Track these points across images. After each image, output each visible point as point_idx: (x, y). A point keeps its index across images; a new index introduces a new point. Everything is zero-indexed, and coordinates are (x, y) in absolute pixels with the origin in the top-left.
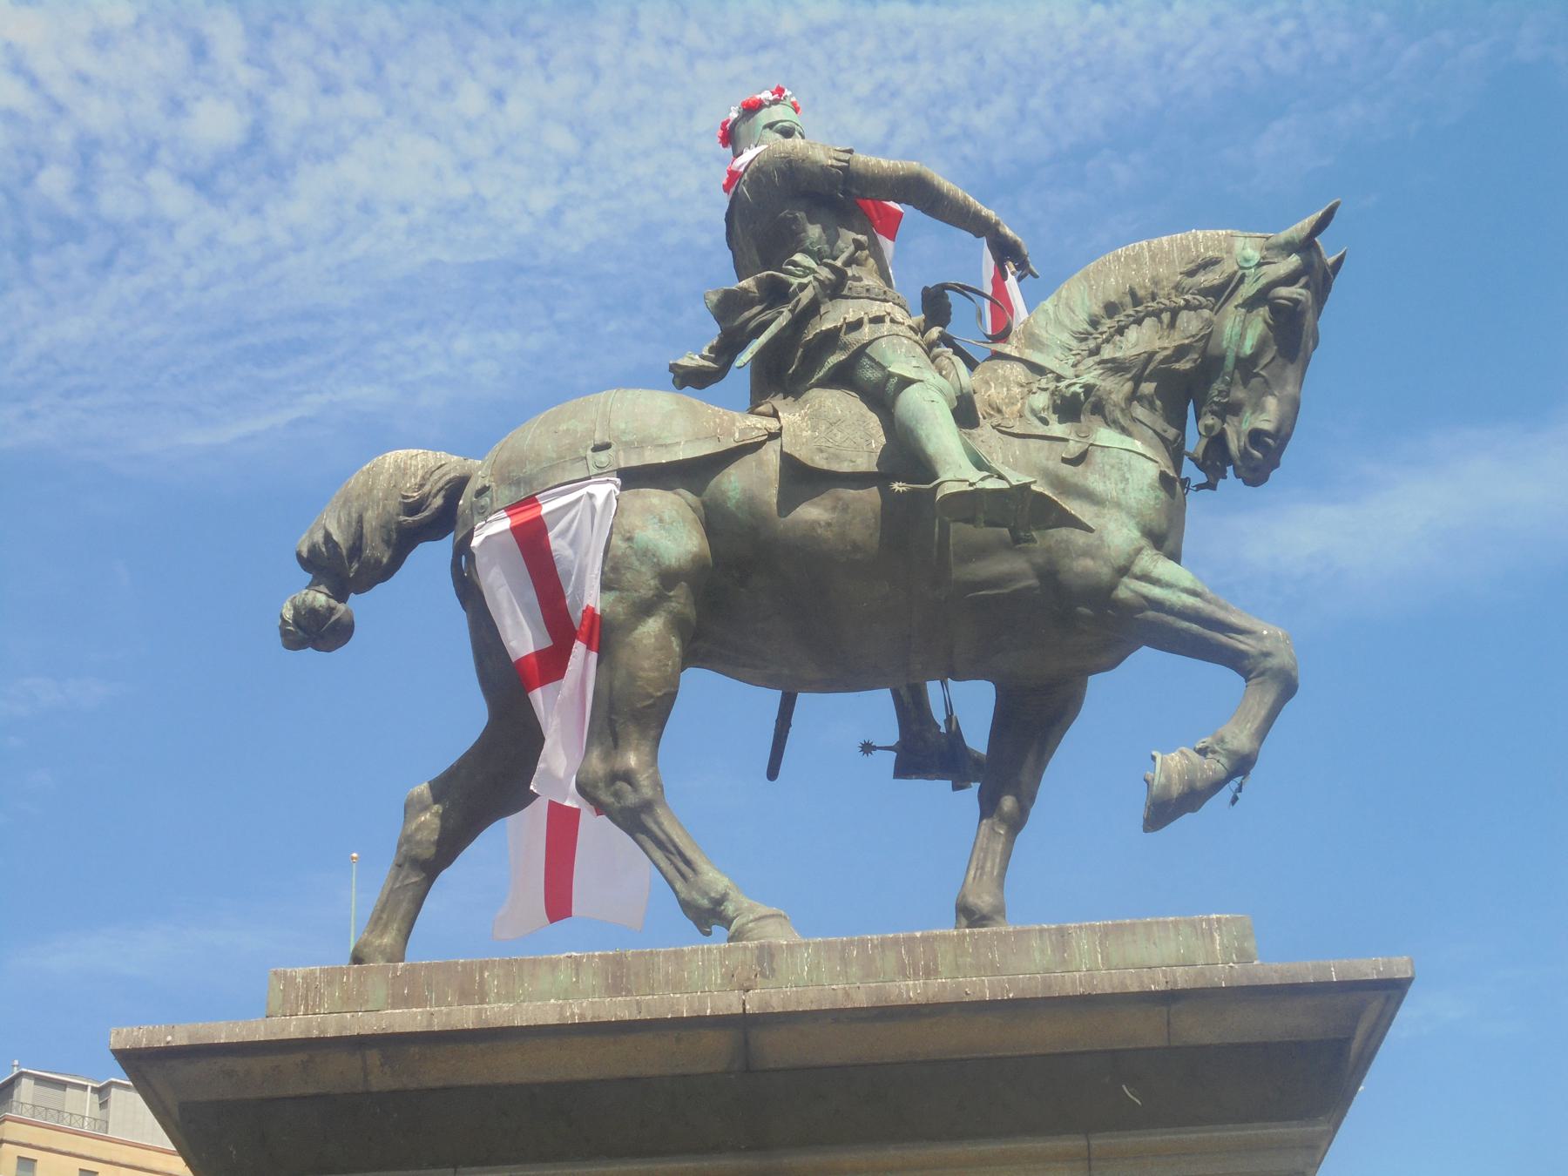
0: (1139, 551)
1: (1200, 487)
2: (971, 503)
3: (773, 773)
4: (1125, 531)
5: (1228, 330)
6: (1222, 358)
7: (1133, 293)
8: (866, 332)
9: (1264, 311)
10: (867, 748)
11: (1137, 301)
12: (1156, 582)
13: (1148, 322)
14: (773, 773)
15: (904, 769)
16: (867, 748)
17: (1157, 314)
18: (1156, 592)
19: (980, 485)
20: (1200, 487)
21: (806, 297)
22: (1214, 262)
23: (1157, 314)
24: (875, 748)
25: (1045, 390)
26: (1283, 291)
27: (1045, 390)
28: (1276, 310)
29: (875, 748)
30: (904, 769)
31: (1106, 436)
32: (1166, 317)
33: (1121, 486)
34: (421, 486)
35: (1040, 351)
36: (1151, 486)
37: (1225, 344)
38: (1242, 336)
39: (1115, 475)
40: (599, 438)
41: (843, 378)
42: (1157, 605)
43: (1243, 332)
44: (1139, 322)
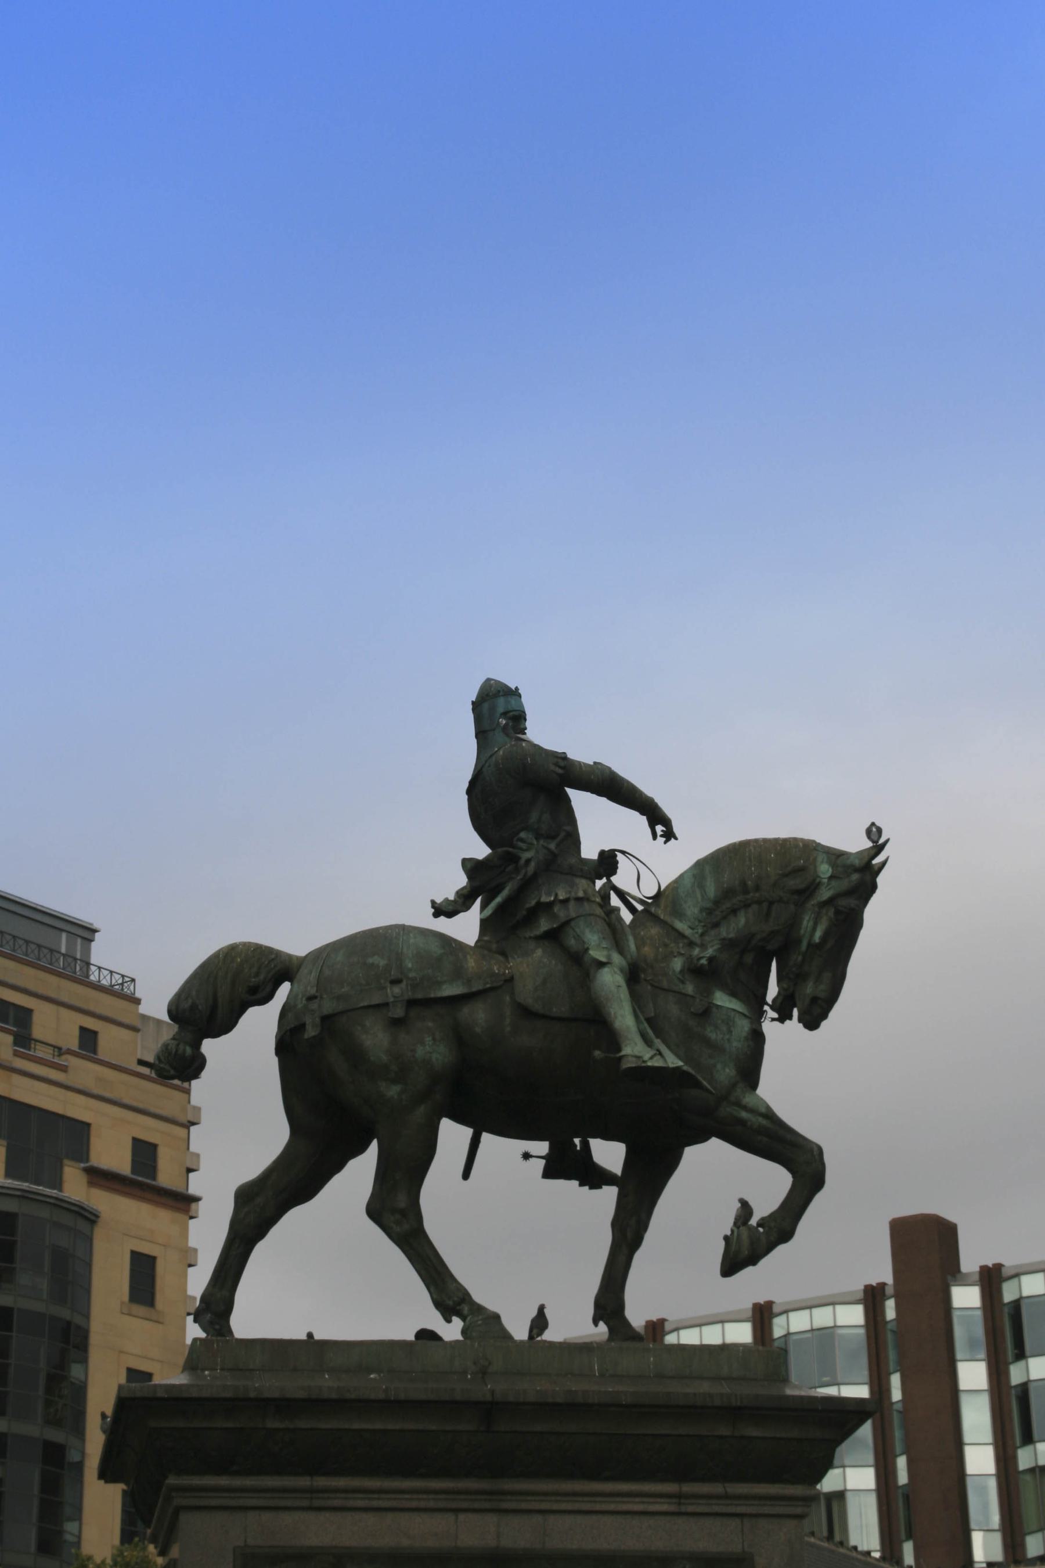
0: (734, 1086)
1: (773, 1020)
2: (643, 1074)
3: (466, 1175)
4: (727, 1070)
5: (805, 922)
6: (799, 941)
7: (743, 883)
8: (573, 910)
9: (831, 912)
10: (527, 1156)
11: (746, 891)
12: (745, 1108)
13: (755, 907)
14: (466, 1175)
15: (549, 1173)
16: (527, 1156)
17: (759, 902)
18: (744, 1114)
19: (649, 1064)
20: (773, 1020)
21: (531, 868)
22: (802, 869)
23: (759, 902)
24: (532, 1156)
25: (682, 954)
26: (843, 902)
27: (682, 954)
28: (837, 912)
29: (532, 1156)
30: (549, 1173)
31: (722, 999)
32: (765, 905)
33: (727, 1037)
34: (257, 974)
35: (681, 921)
36: (746, 1039)
37: (802, 932)
38: (814, 929)
39: (724, 1028)
40: (394, 974)
41: (553, 936)
42: (742, 1122)
43: (814, 929)
44: (747, 906)
